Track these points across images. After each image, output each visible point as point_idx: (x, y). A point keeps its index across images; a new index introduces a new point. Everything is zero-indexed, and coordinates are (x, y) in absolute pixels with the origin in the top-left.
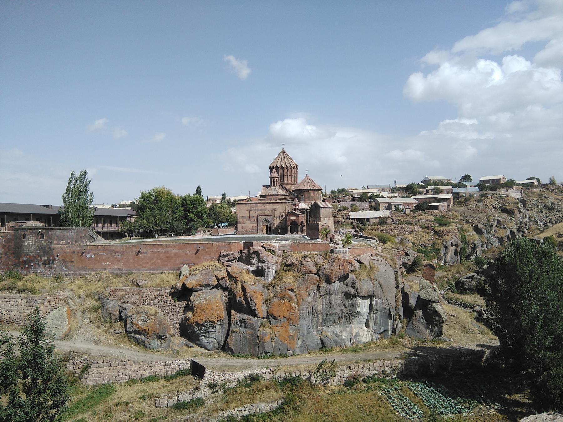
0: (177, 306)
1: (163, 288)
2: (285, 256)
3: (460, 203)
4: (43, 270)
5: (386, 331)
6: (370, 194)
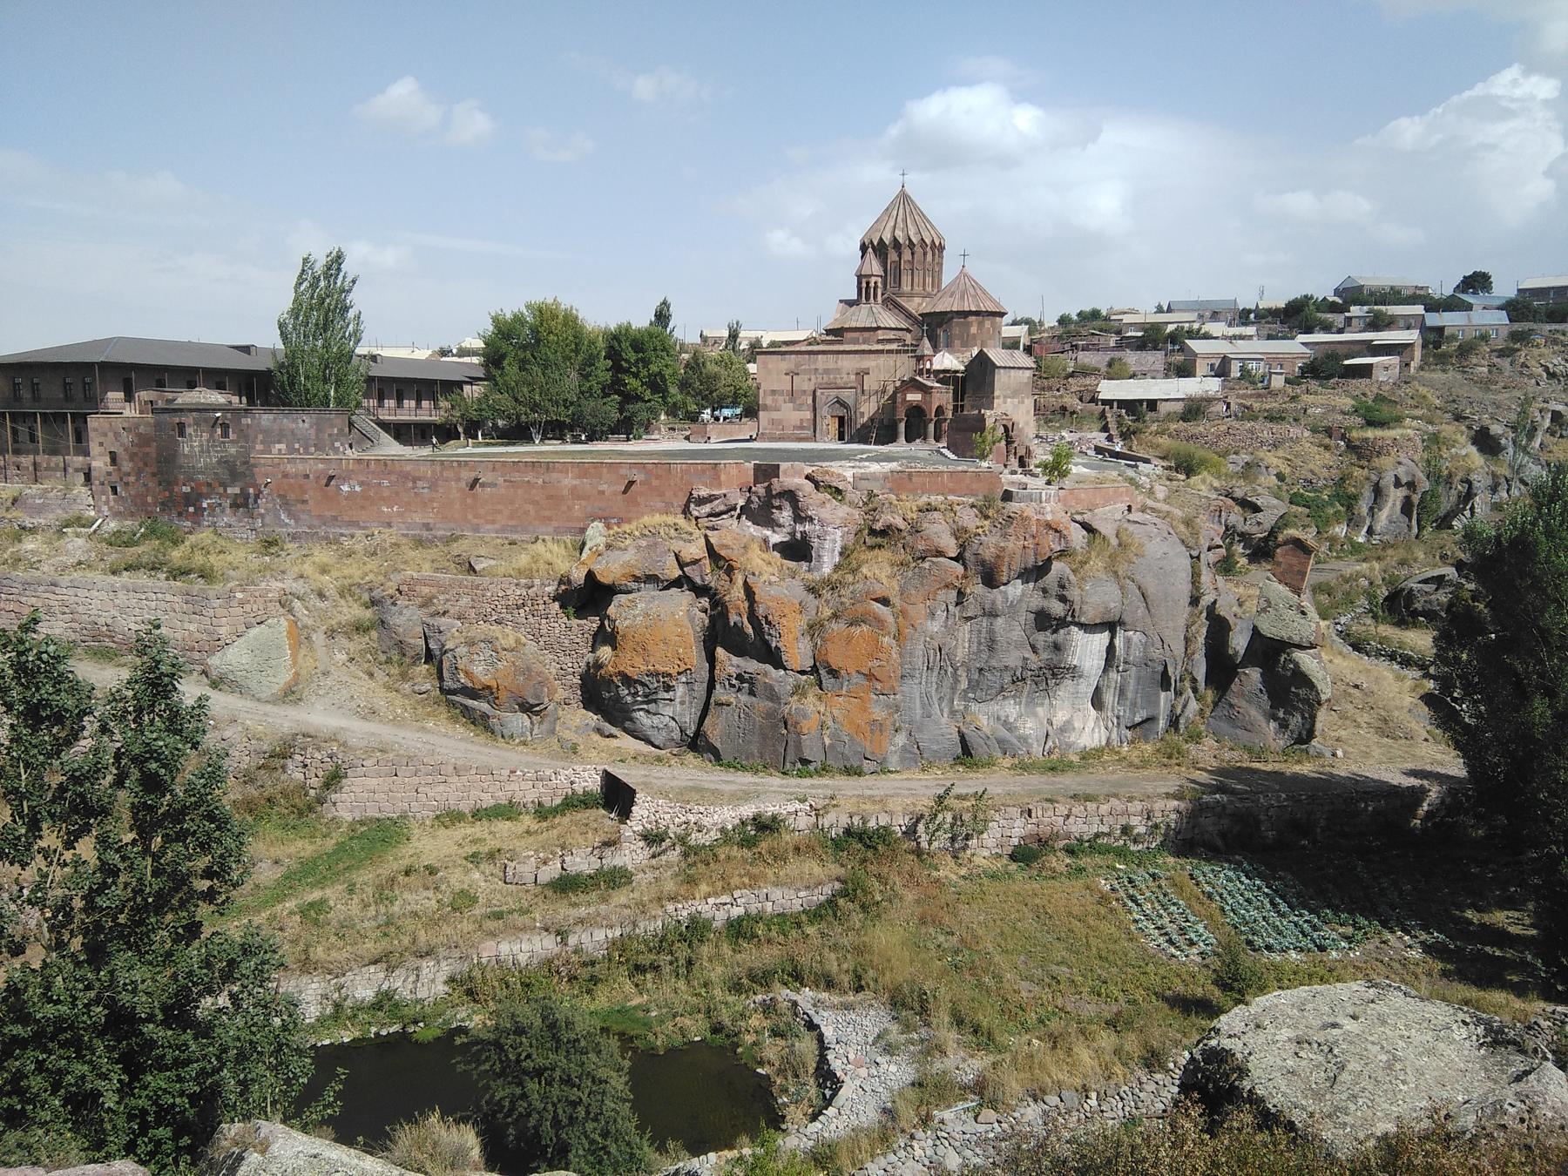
0: (575, 629)
1: (537, 582)
2: (871, 505)
3: (1442, 359)
4: (233, 521)
5: (1151, 720)
6: (1171, 328)
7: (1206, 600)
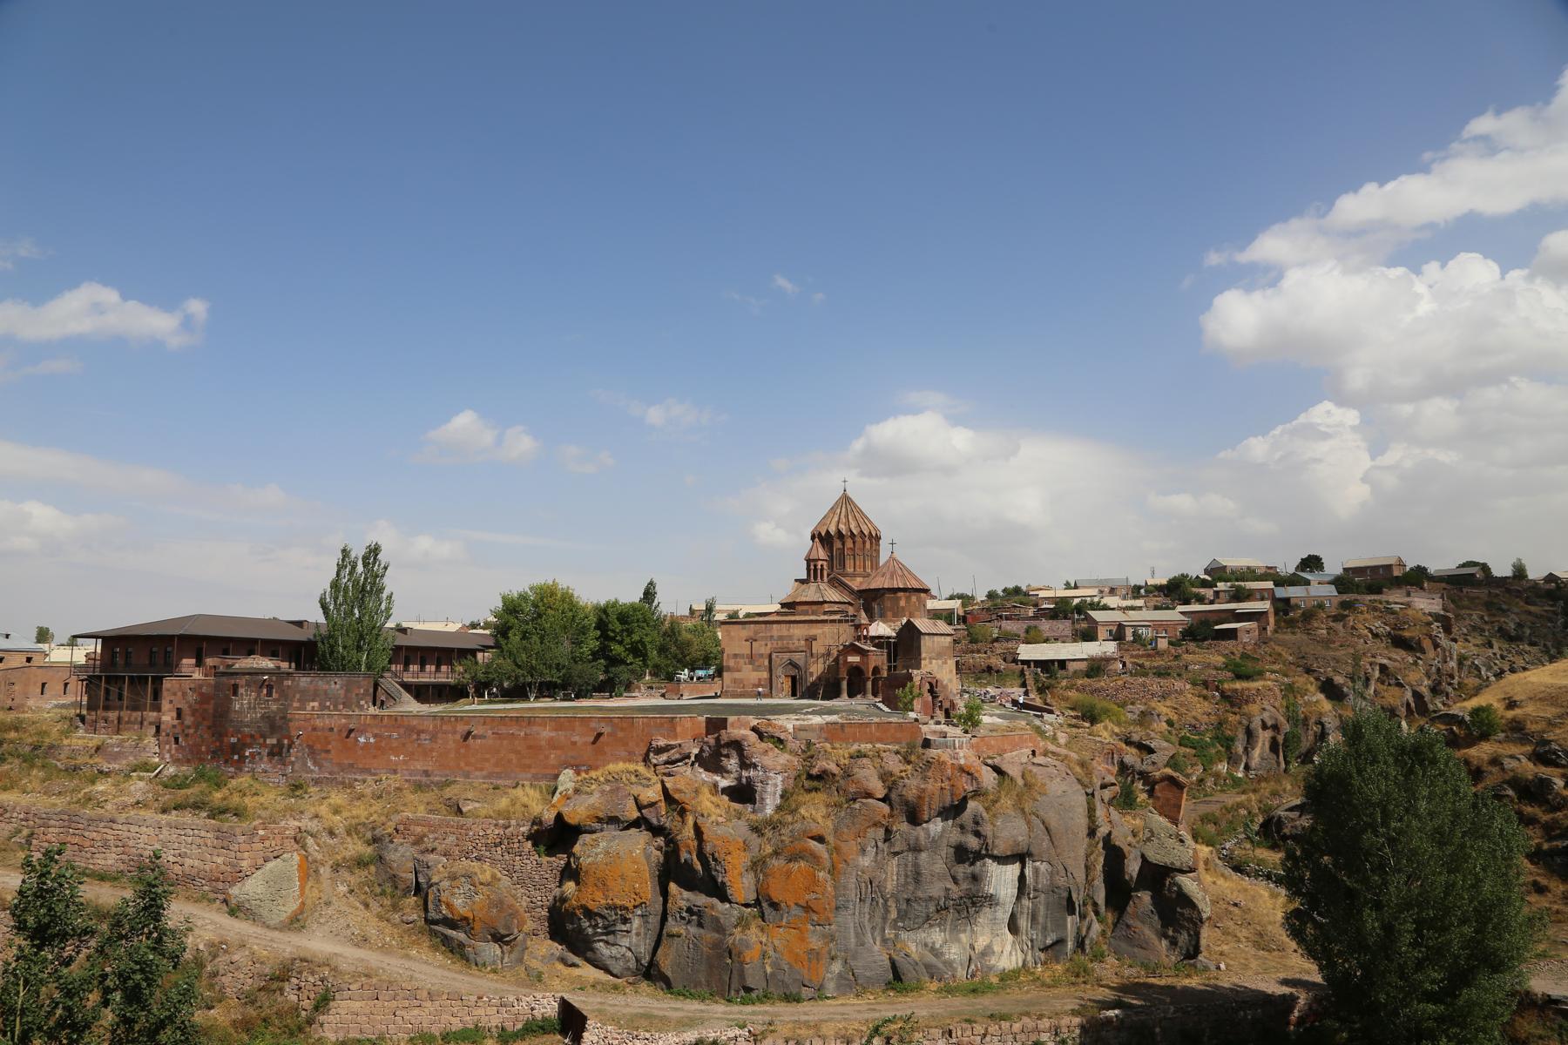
1: (513, 822)
5: (1060, 942)
7: (1102, 831)
